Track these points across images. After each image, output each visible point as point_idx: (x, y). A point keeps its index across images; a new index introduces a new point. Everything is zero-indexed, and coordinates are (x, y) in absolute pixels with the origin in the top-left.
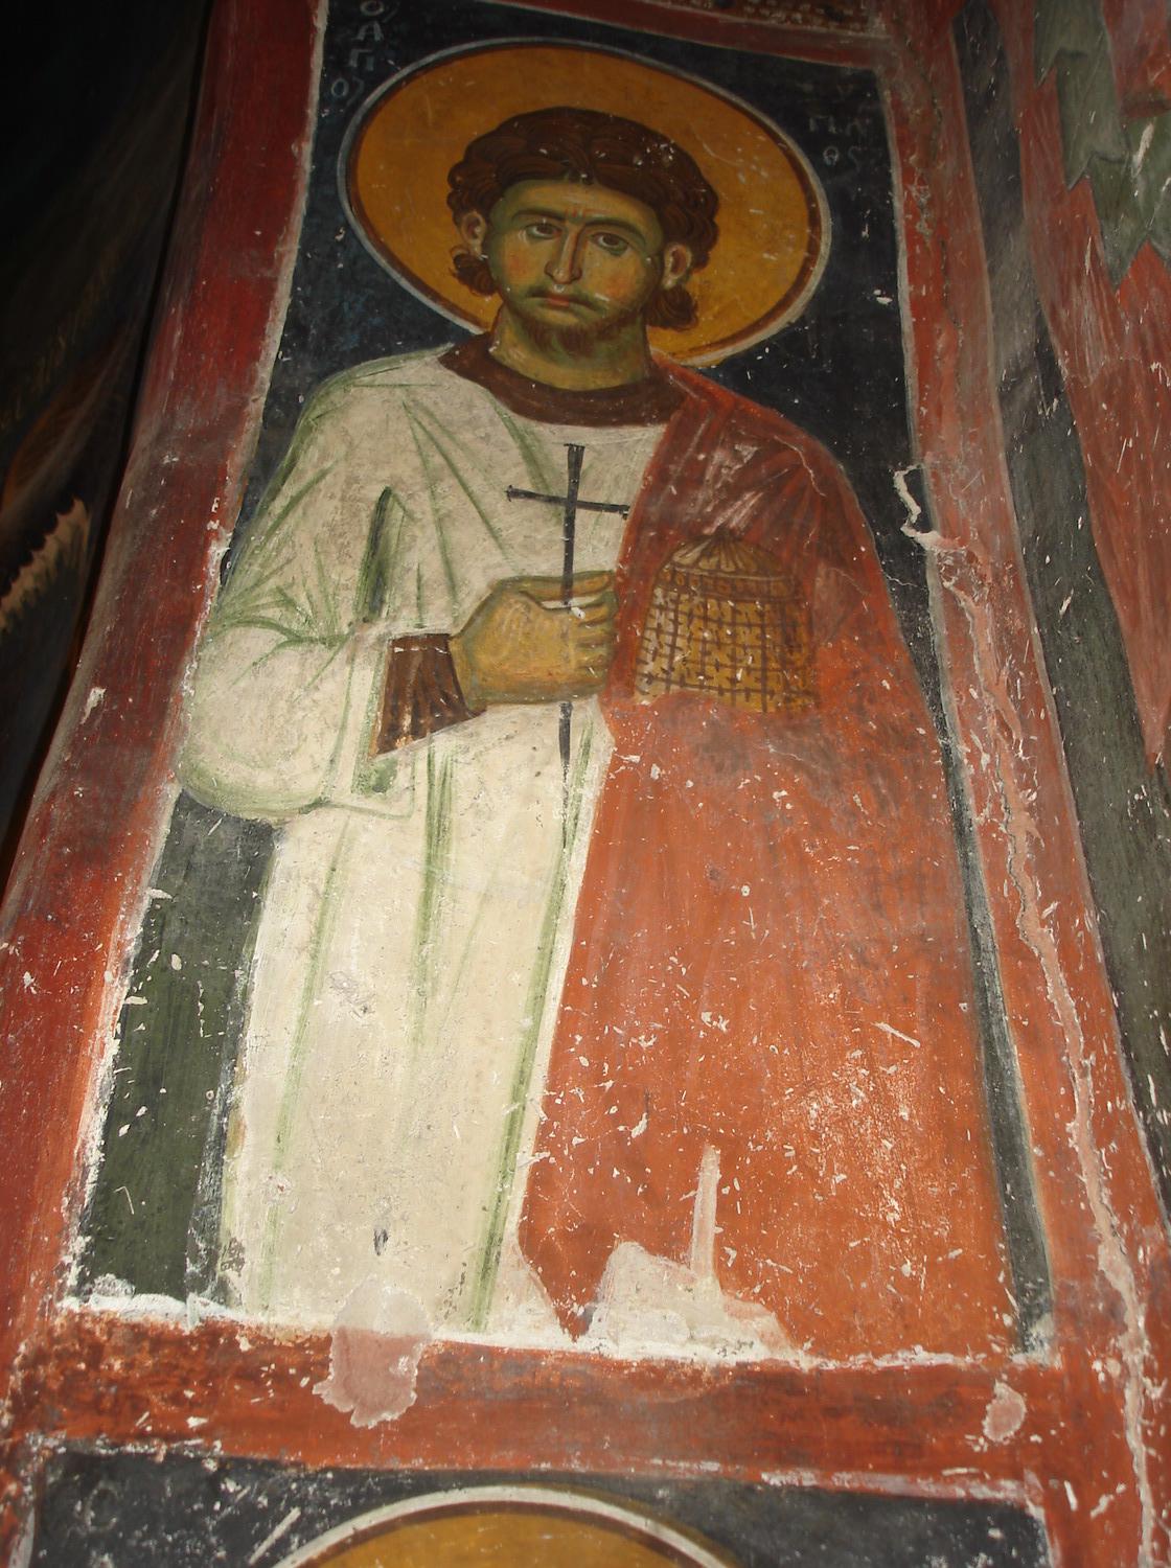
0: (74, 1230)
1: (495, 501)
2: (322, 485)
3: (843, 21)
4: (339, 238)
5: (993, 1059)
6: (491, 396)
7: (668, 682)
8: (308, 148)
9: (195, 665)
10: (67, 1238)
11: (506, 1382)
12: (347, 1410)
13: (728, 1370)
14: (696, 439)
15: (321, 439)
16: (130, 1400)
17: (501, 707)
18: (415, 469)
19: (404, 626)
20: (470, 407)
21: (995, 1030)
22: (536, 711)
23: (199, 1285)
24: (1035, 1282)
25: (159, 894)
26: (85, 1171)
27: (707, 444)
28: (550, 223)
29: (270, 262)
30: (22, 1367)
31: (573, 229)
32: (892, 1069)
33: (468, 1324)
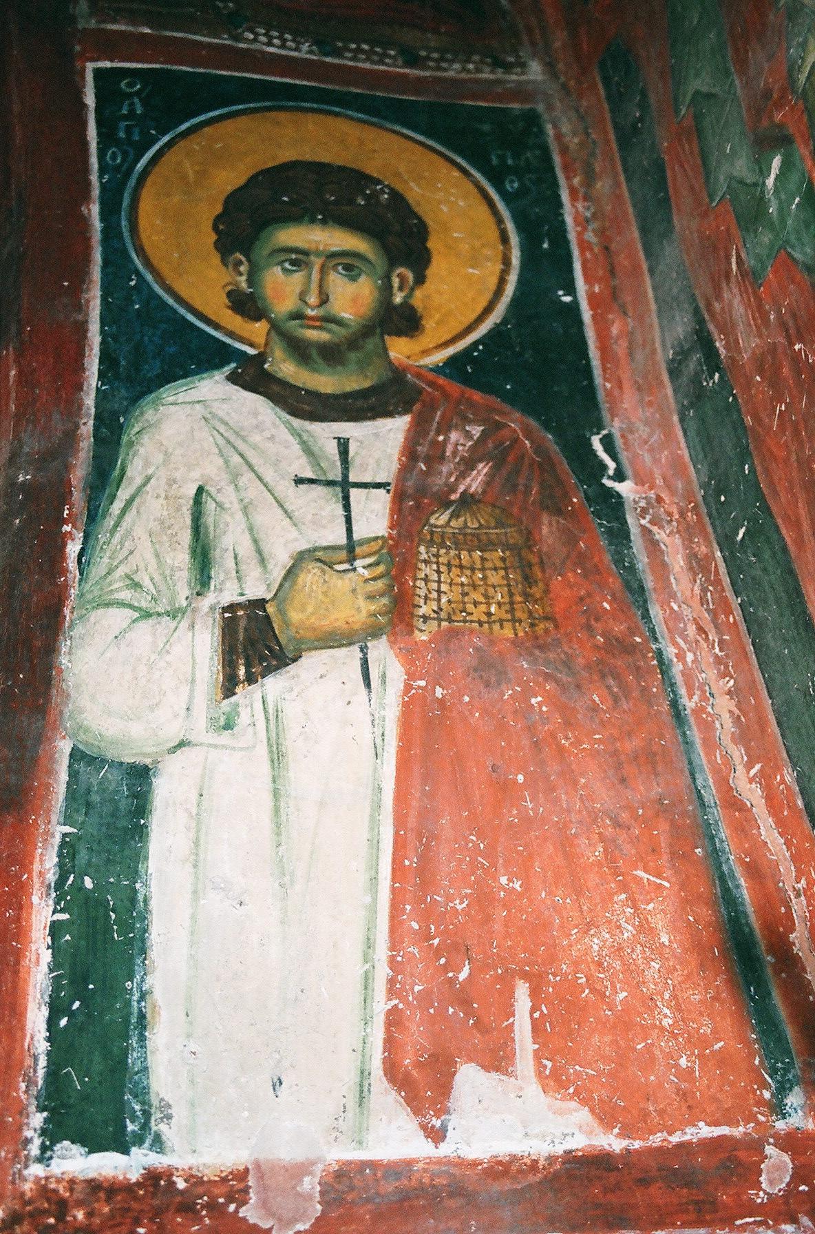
0: (33, 1108)
1: (286, 489)
2: (148, 488)
3: (508, 67)
4: (133, 283)
7: (440, 620)
8: (95, 209)
9: (68, 643)
10: (28, 1117)
11: (389, 1187)
12: (267, 1226)
13: (558, 1157)
14: (435, 424)
15: (142, 450)
17: (314, 653)
19: (229, 595)
20: (256, 414)
21: (725, 868)
22: (341, 652)
23: (139, 1140)
24: (783, 1063)
25: (68, 829)
26: (36, 1058)
27: (445, 428)
28: (298, 259)
29: (80, 307)
31: (317, 262)
32: (651, 907)
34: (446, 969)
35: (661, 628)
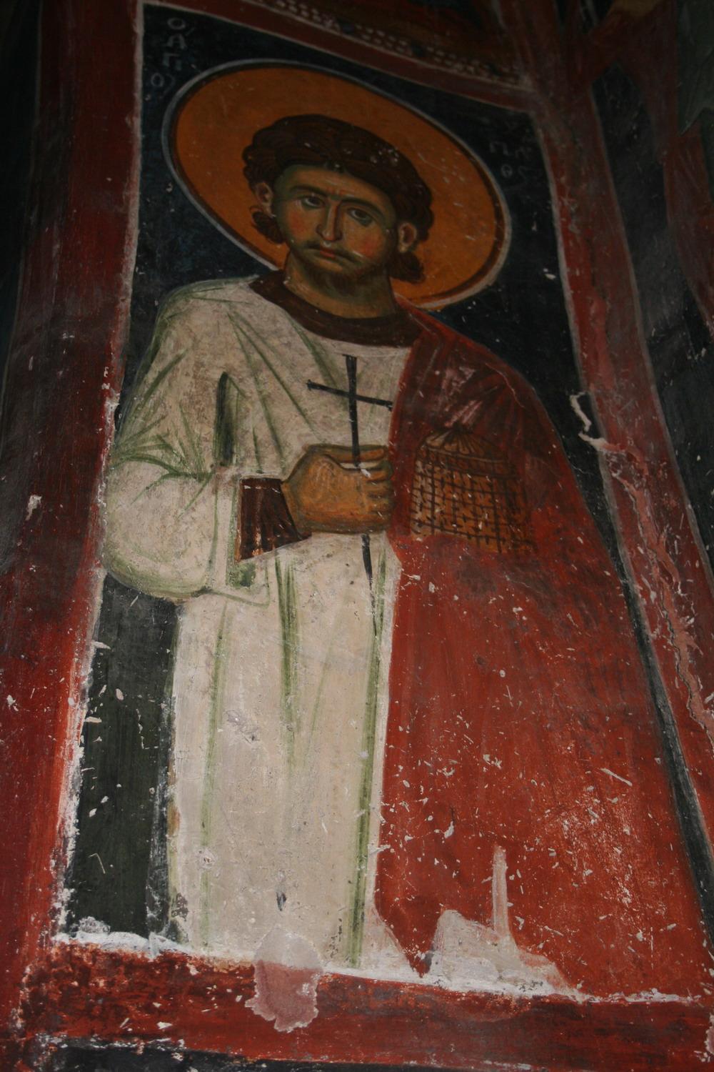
0: (61, 884)
2: (179, 365)
3: (503, 76)
5: (681, 797)
6: (289, 316)
7: (433, 527)
8: (138, 122)
9: (104, 485)
10: (56, 890)
11: (379, 1003)
12: (271, 1019)
13: (527, 1001)
14: (432, 361)
15: (174, 333)
16: (113, 1008)
17: (322, 534)
18: (242, 362)
19: (249, 471)
20: (275, 321)
21: (680, 777)
22: (346, 539)
23: (158, 929)
25: (101, 645)
26: (66, 840)
27: (441, 364)
28: (318, 198)
29: (123, 202)
30: (29, 985)
32: (615, 800)
33: (347, 962)
34: (433, 825)
35: (628, 567)
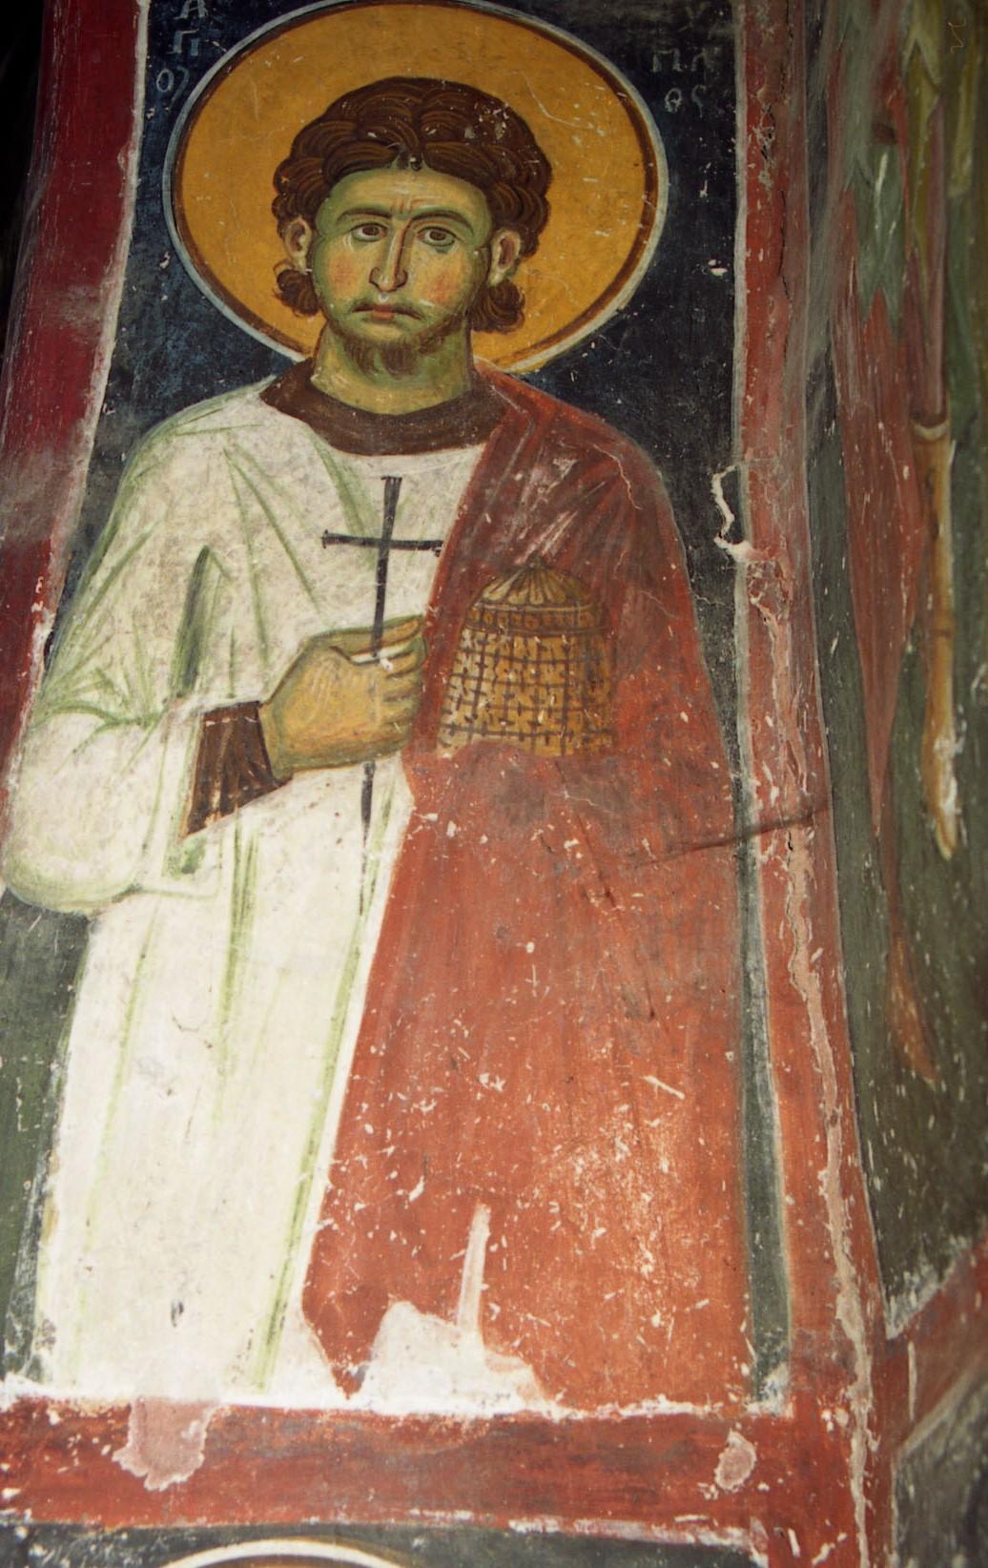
1: (309, 548)
2: (142, 552)
4: (164, 265)
5: (754, 1107)
6: (310, 431)
7: (471, 731)
8: (134, 157)
11: (284, 1441)
14: (514, 457)
15: (142, 500)
17: (308, 774)
18: (234, 522)
20: (290, 446)
21: (758, 1078)
22: (338, 775)
23: (16, 1364)
27: (525, 463)
28: (373, 223)
32: (655, 1123)
34: (395, 1184)
35: (746, 748)
